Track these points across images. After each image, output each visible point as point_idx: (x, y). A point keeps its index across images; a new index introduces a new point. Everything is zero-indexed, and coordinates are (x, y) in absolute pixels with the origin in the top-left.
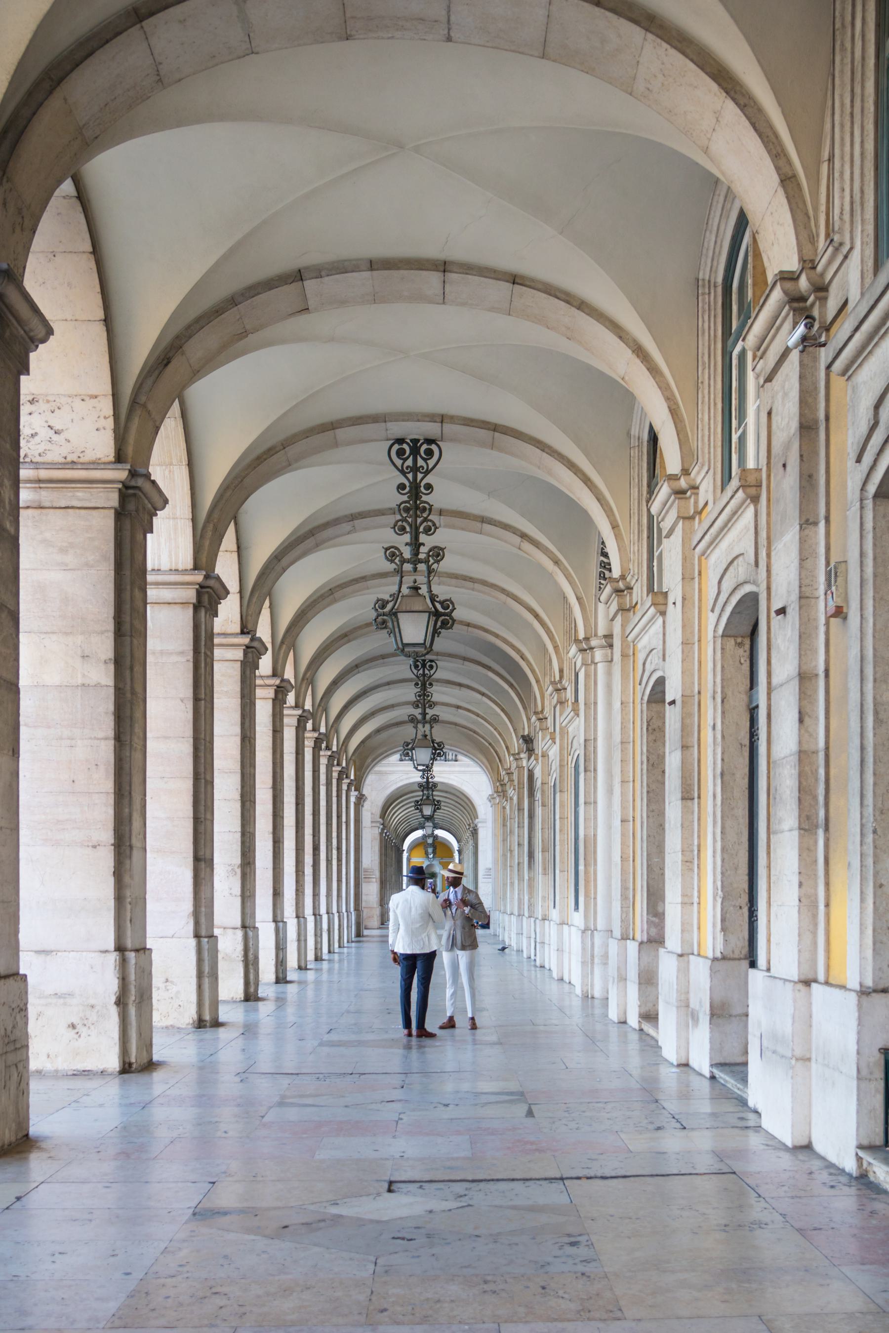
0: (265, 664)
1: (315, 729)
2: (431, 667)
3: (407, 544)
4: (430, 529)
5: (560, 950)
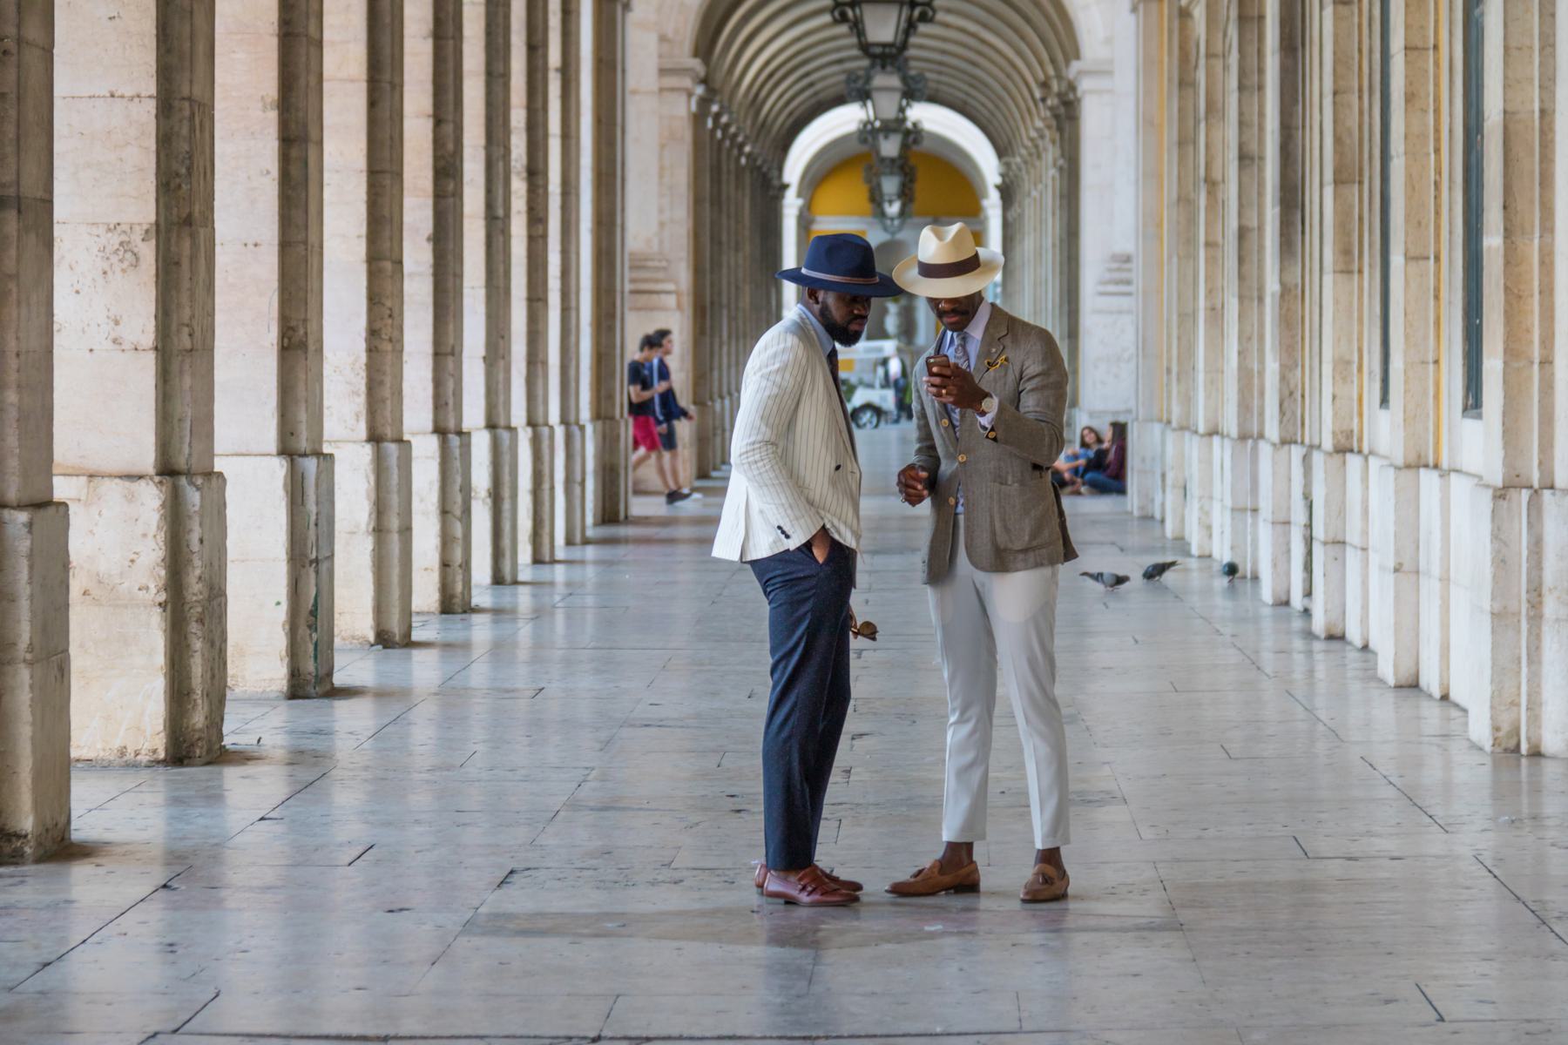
5: (1406, 570)
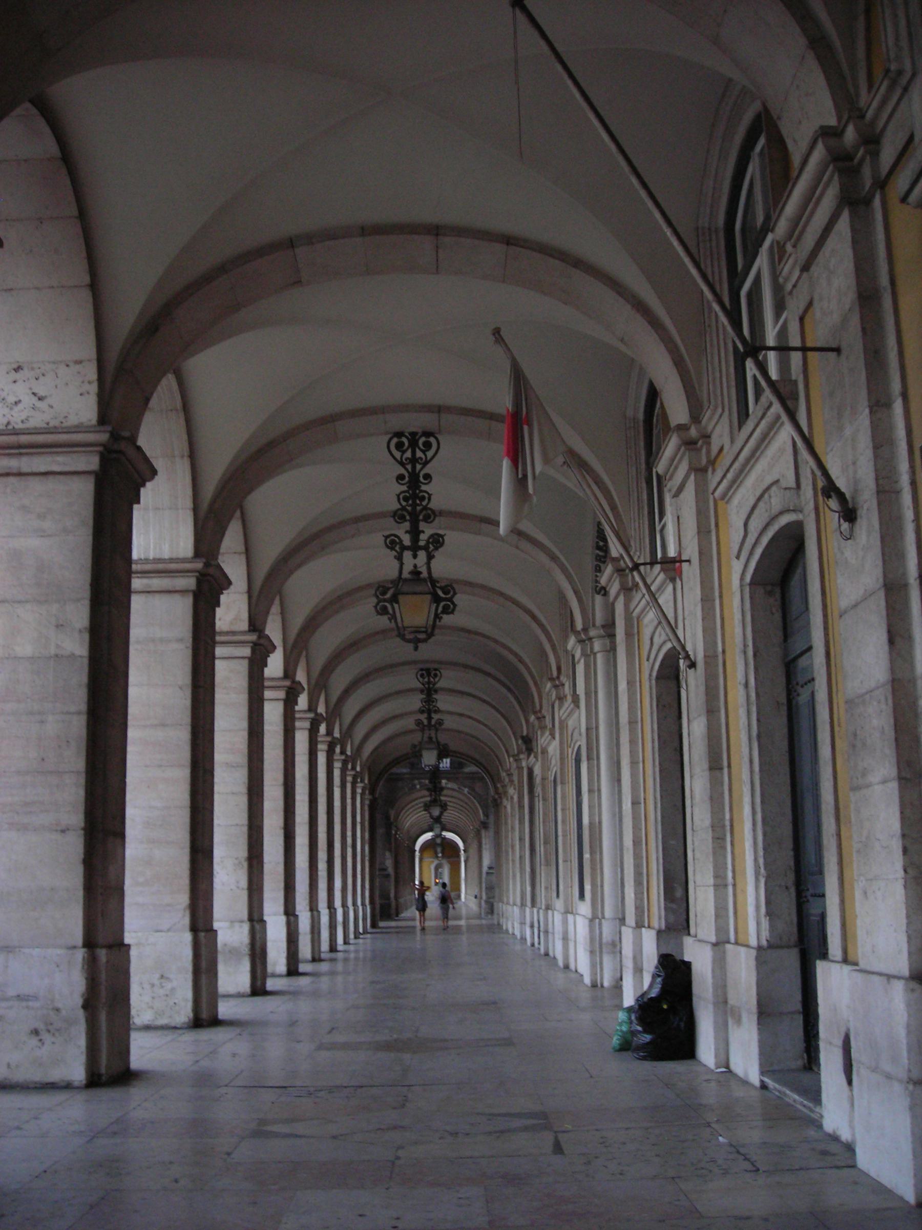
0: (303, 702)
1: (343, 752)
2: (436, 675)
3: (407, 532)
4: (429, 517)
5: (565, 939)
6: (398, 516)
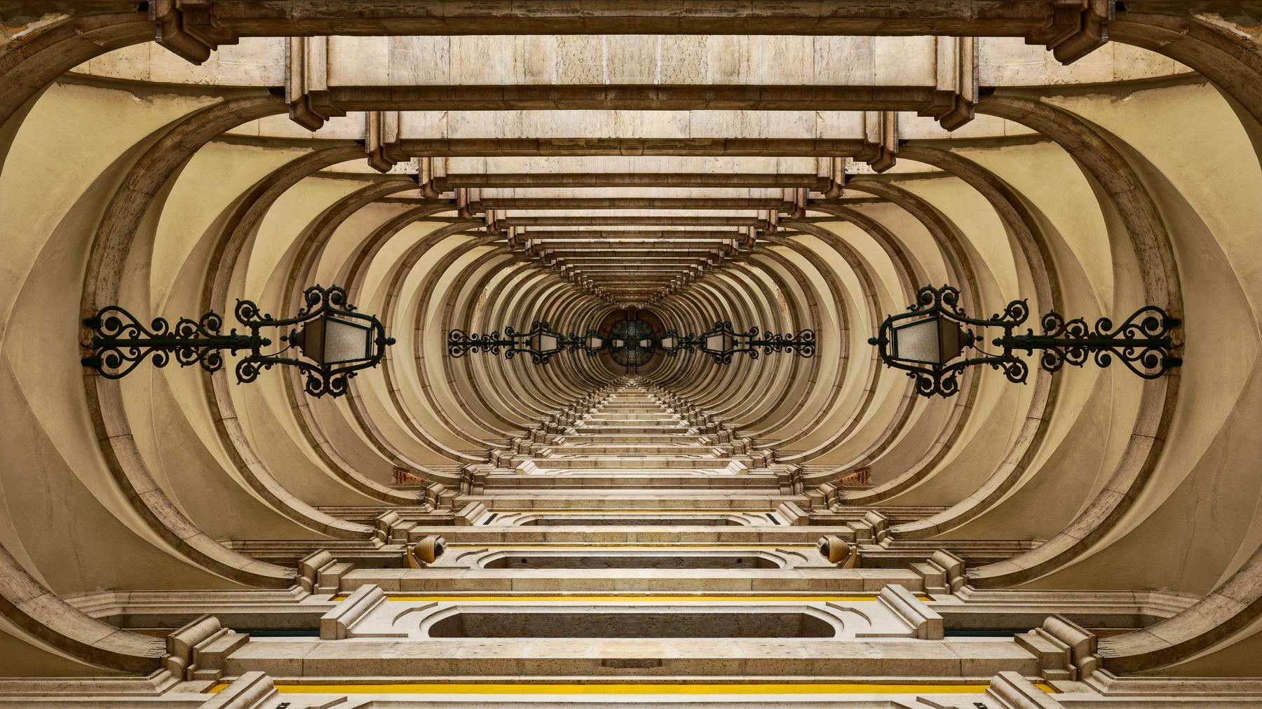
3: (234, 354)
6: (212, 365)
